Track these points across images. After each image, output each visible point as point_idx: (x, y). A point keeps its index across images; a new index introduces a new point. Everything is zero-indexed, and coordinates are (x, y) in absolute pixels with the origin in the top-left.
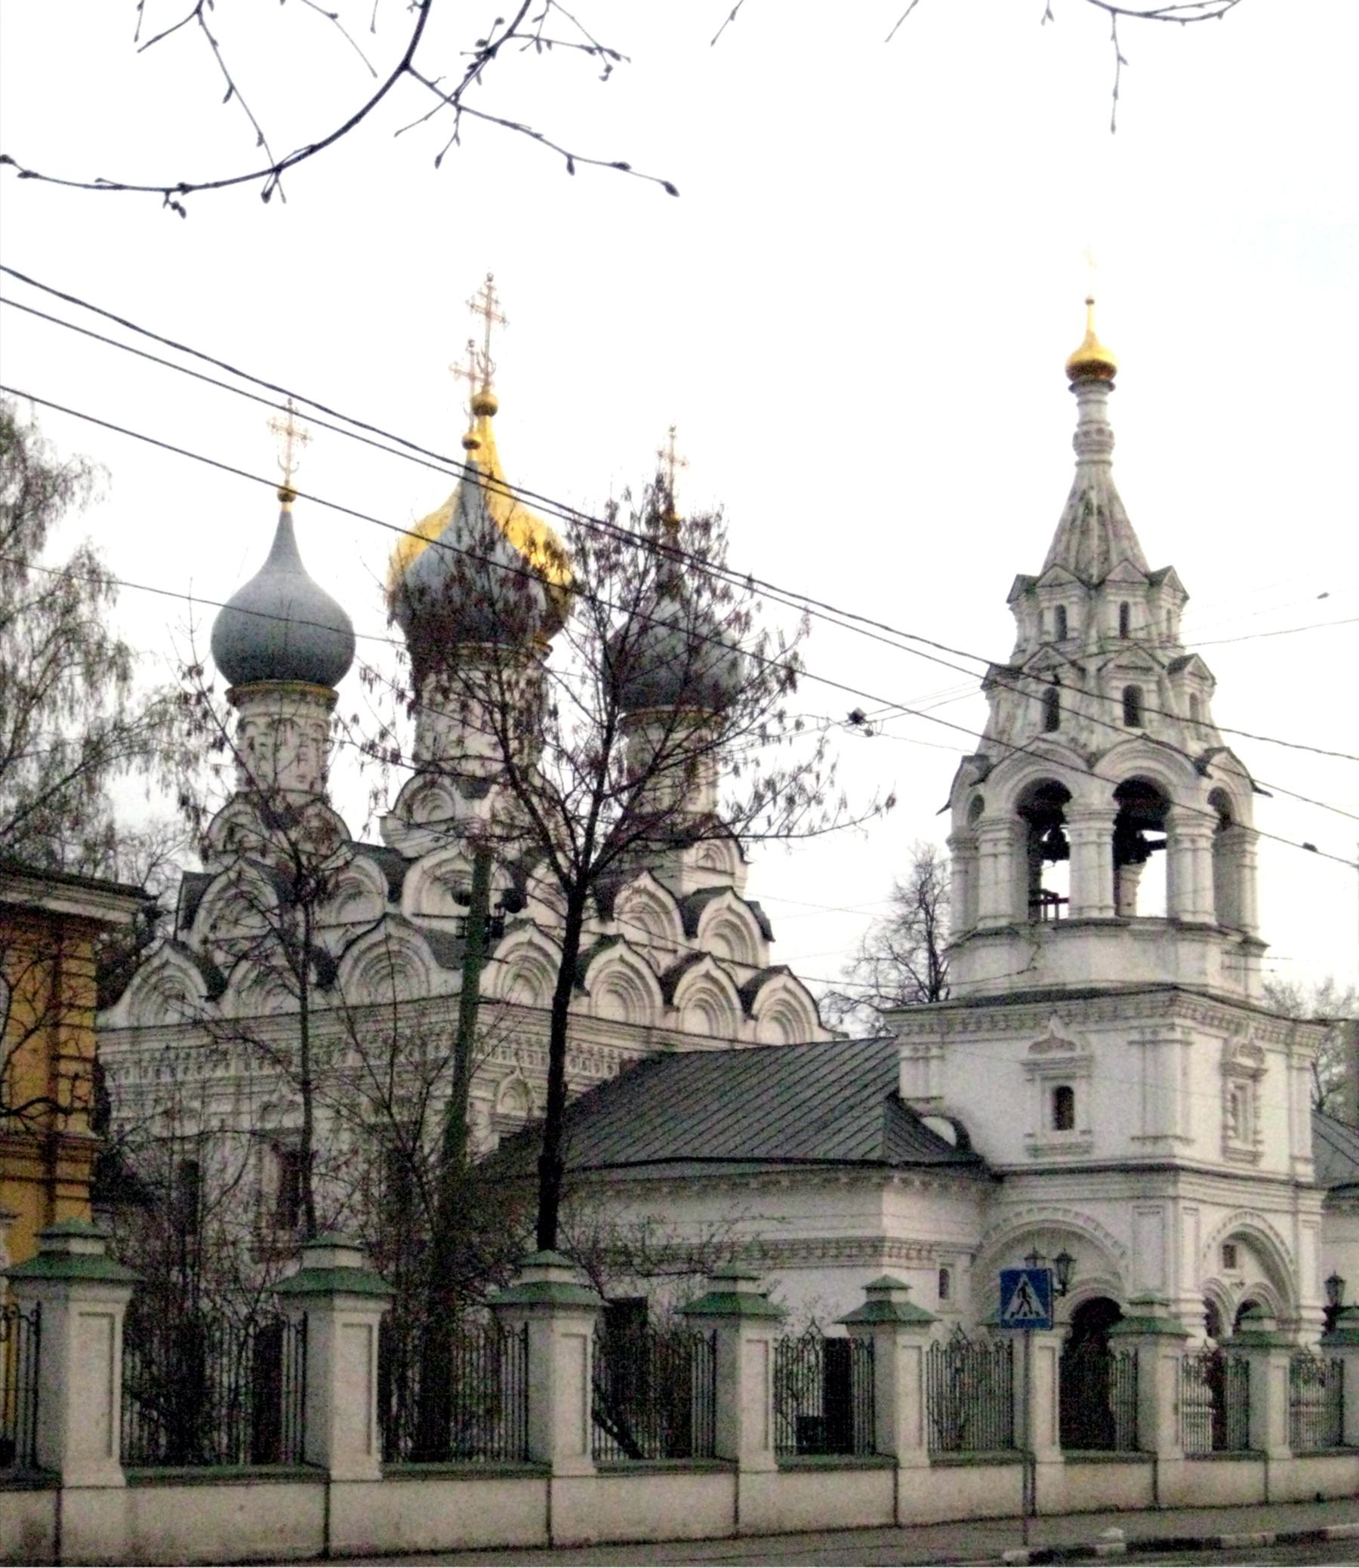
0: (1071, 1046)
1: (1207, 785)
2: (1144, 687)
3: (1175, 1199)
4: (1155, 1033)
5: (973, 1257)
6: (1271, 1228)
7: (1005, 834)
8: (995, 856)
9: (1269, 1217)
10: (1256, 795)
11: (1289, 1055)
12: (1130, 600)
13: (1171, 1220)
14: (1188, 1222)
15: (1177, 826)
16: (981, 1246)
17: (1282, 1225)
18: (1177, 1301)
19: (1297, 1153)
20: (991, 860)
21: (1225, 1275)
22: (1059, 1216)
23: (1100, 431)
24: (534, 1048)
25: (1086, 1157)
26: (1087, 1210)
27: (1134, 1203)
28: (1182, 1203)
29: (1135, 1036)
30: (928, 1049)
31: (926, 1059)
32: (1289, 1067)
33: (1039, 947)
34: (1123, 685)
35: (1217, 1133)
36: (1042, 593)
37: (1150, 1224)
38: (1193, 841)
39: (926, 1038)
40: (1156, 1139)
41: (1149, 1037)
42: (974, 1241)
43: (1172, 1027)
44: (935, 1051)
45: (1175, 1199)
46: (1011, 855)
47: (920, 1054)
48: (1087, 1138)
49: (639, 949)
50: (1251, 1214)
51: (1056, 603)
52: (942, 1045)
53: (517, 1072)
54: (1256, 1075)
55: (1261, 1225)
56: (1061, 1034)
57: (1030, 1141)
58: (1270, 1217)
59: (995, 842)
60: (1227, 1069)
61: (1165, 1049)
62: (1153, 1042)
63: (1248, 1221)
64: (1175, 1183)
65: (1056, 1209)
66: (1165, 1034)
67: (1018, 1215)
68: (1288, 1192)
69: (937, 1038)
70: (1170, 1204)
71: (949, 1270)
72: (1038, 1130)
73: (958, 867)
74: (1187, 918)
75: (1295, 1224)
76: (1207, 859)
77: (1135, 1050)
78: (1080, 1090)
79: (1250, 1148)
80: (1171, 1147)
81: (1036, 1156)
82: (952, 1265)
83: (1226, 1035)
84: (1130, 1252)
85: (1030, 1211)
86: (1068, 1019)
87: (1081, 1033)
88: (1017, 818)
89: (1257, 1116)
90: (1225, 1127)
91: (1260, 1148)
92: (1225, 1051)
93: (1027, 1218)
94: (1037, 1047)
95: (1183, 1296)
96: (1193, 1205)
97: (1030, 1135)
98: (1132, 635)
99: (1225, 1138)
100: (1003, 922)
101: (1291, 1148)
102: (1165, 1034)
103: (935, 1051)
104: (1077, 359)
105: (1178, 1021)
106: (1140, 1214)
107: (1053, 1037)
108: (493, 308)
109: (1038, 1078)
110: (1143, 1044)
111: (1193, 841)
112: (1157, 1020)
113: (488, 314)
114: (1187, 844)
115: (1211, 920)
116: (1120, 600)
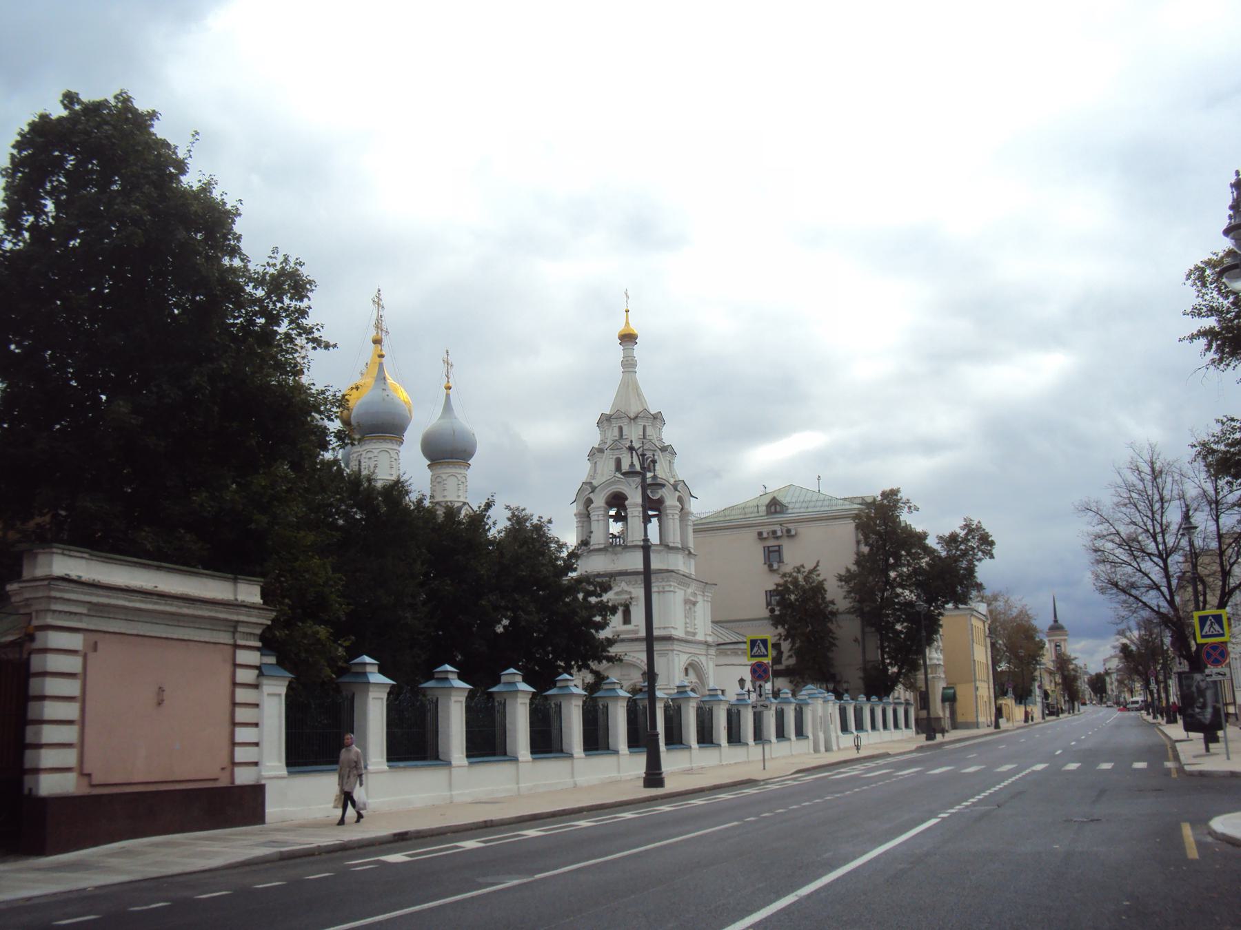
3: (672, 650)
4: (664, 588)
7: (602, 512)
8: (598, 520)
9: (699, 656)
10: (692, 498)
12: (647, 424)
14: (676, 659)
17: (703, 659)
19: (707, 633)
20: (596, 522)
23: (632, 360)
25: (636, 636)
28: (675, 652)
32: (704, 600)
36: (614, 421)
40: (664, 628)
41: (661, 589)
48: (637, 628)
51: (617, 425)
54: (694, 604)
55: (697, 660)
56: (627, 588)
58: (701, 657)
59: (598, 515)
60: (687, 602)
62: (664, 592)
68: (704, 647)
73: (580, 525)
74: (671, 545)
75: (707, 660)
76: (677, 522)
79: (692, 630)
80: (670, 631)
82: (585, 677)
83: (685, 588)
86: (628, 583)
88: (606, 506)
89: (695, 619)
90: (686, 623)
91: (697, 631)
96: (677, 653)
98: (648, 438)
99: (686, 627)
100: (602, 546)
102: (667, 589)
104: (623, 333)
105: (672, 583)
107: (623, 590)
112: (664, 583)
113: (378, 304)
114: (671, 517)
115: (680, 546)
116: (643, 424)
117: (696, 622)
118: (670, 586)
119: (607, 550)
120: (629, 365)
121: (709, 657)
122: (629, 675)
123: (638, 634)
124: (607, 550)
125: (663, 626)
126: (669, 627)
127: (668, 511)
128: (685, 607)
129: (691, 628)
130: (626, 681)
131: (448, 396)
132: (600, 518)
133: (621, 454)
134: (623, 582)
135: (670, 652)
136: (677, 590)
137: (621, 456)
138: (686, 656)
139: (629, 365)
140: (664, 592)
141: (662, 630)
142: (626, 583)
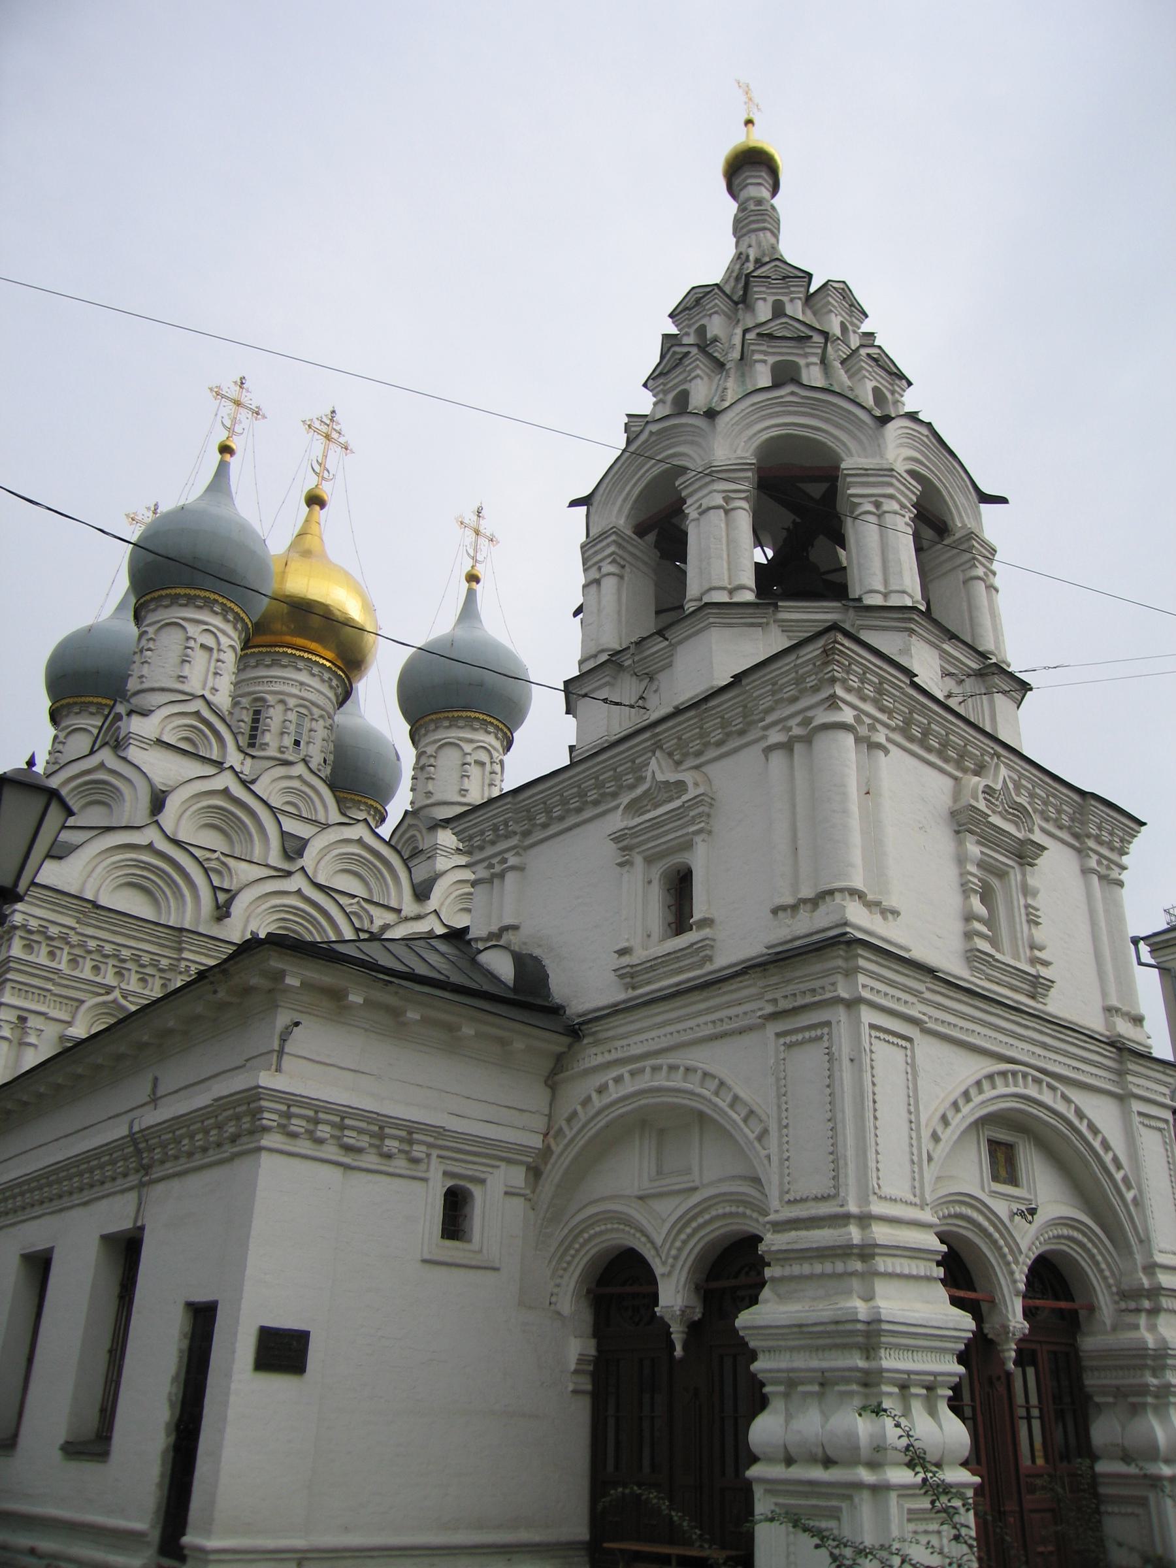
0: (681, 786)
2: (802, 362)
3: (853, 1004)
5: (535, 1173)
6: (1080, 1114)
10: (983, 506)
11: (1081, 852)
13: (845, 1049)
16: (546, 1152)
18: (865, 1220)
21: (994, 1194)
22: (661, 1081)
24: (149, 970)
25: (709, 967)
26: (700, 1057)
27: (772, 1028)
28: (868, 1016)
29: (776, 737)
30: (505, 861)
31: (501, 876)
32: (1086, 871)
33: (651, 679)
34: (771, 360)
35: (957, 927)
37: (809, 1060)
38: (878, 505)
42: (536, 1141)
43: (833, 702)
44: (512, 860)
45: (853, 1004)
46: (621, 577)
48: (706, 932)
49: (343, 900)
50: (1037, 1081)
52: (518, 850)
53: (116, 994)
54: (1026, 854)
57: (626, 960)
61: (823, 741)
63: (1032, 1091)
64: (851, 973)
65: (655, 1069)
66: (823, 717)
67: (601, 1090)
69: (514, 841)
70: (841, 1013)
71: (476, 1191)
72: (636, 943)
78: (700, 861)
81: (634, 988)
82: (482, 1182)
84: (773, 1127)
85: (618, 1080)
87: (697, 767)
89: (1033, 922)
90: (969, 917)
92: (957, 795)
93: (614, 1093)
94: (634, 807)
95: (877, 1208)
97: (623, 952)
99: (969, 935)
101: (1104, 994)
102: (823, 717)
103: (512, 860)
106: (789, 1046)
108: (335, 435)
109: (639, 860)
110: (787, 747)
111: (878, 505)
117: (1039, 935)
119: (620, 667)
121: (1137, 1106)
122: (688, 1171)
123: (710, 959)
125: (807, 892)
128: (960, 843)
129: (1016, 956)
130: (672, 1202)
131: (471, 594)
132: (605, 570)
134: (658, 753)
138: (973, 1068)
140: (808, 740)
142: (670, 755)
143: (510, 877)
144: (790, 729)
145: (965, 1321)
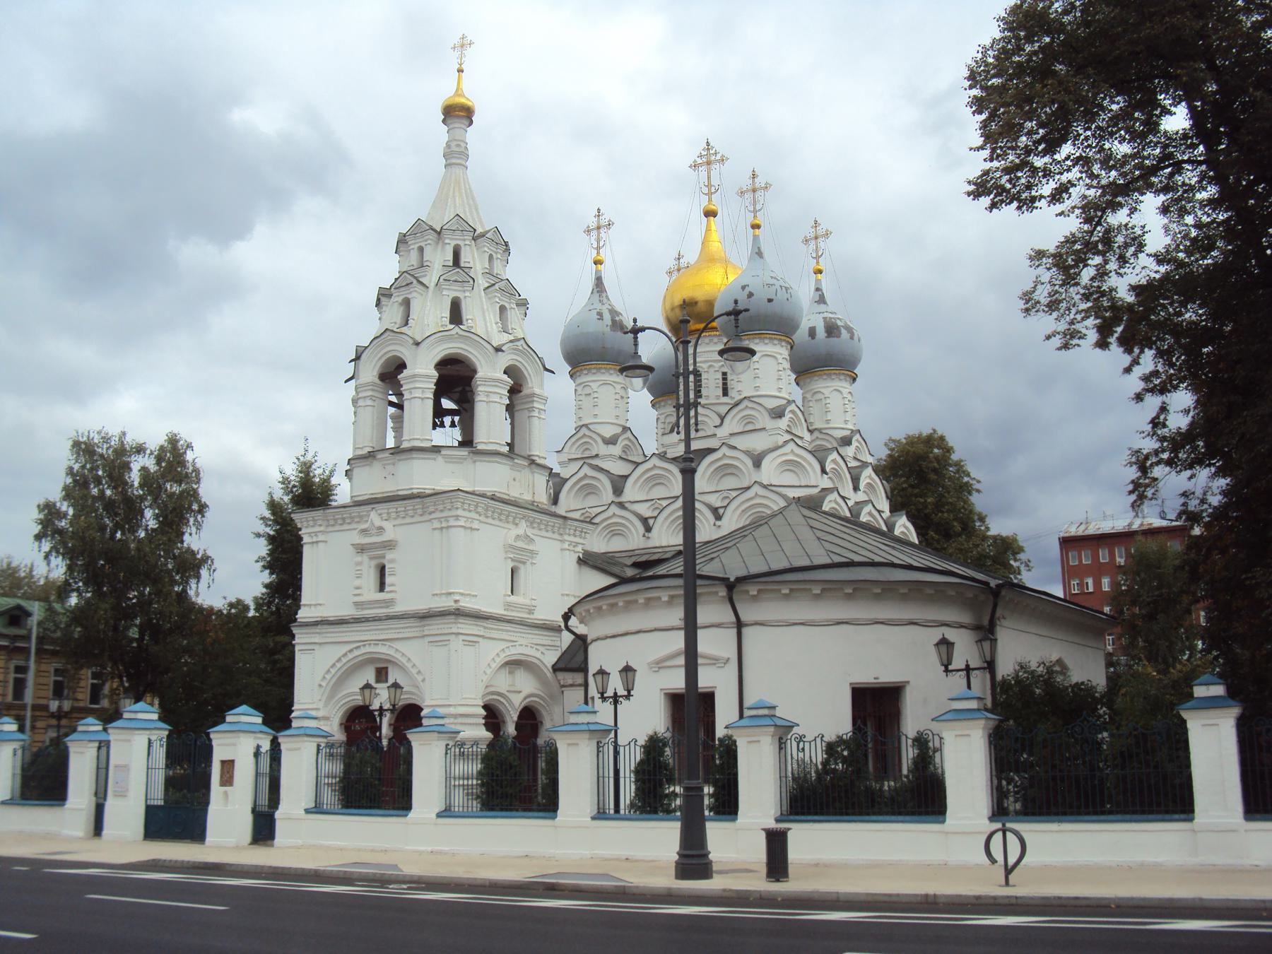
1: (505, 360)
15: (478, 385)
39: (317, 529)
41: (444, 525)
46: (374, 406)
47: (315, 539)
69: (322, 529)
77: (437, 532)
79: (527, 602)
88: (378, 381)
116: (454, 243)
118: (457, 517)
120: (455, 155)
124: (374, 457)
126: (453, 593)
127: (480, 389)
133: (411, 293)
135: (452, 637)
136: (476, 525)
137: (409, 296)
139: (455, 155)
140: (449, 527)
141: (444, 598)
143: (321, 545)
144: (441, 522)
145: (489, 735)
